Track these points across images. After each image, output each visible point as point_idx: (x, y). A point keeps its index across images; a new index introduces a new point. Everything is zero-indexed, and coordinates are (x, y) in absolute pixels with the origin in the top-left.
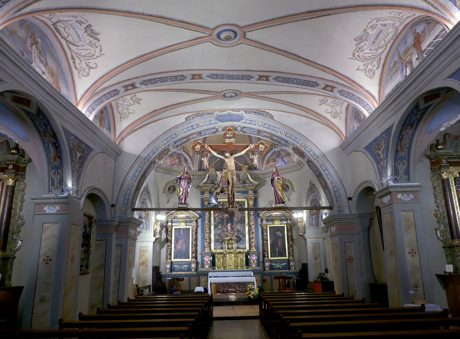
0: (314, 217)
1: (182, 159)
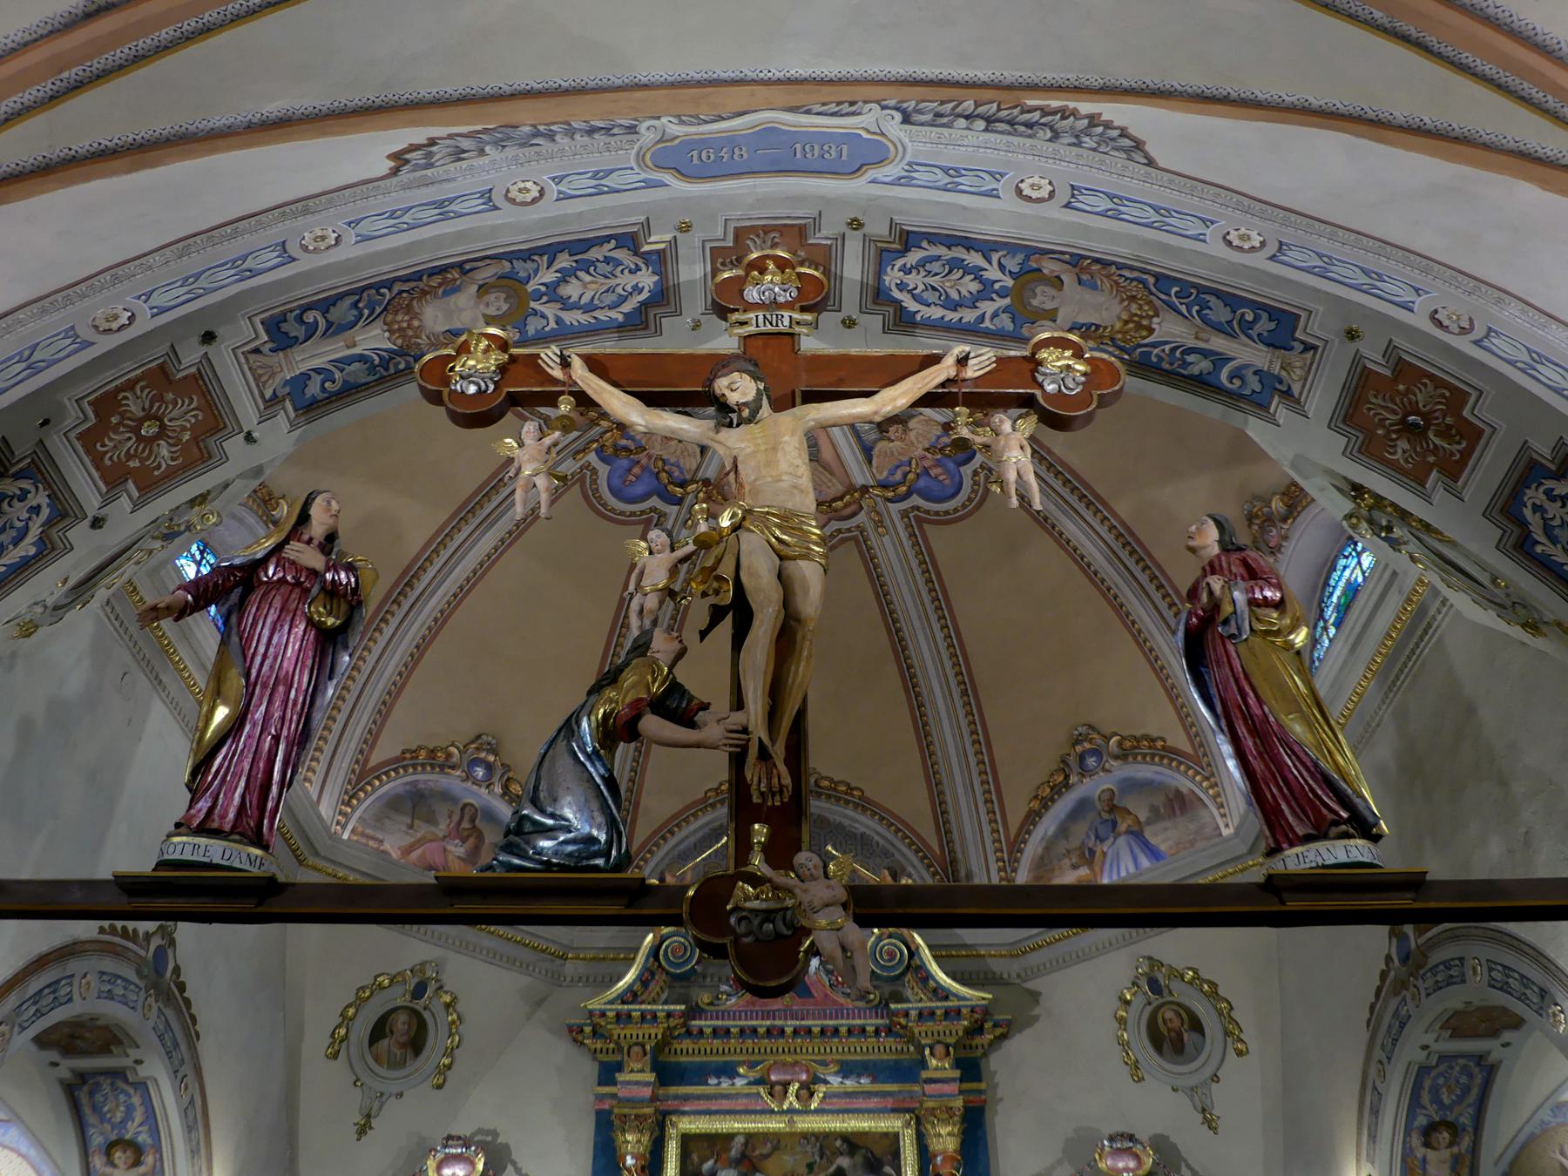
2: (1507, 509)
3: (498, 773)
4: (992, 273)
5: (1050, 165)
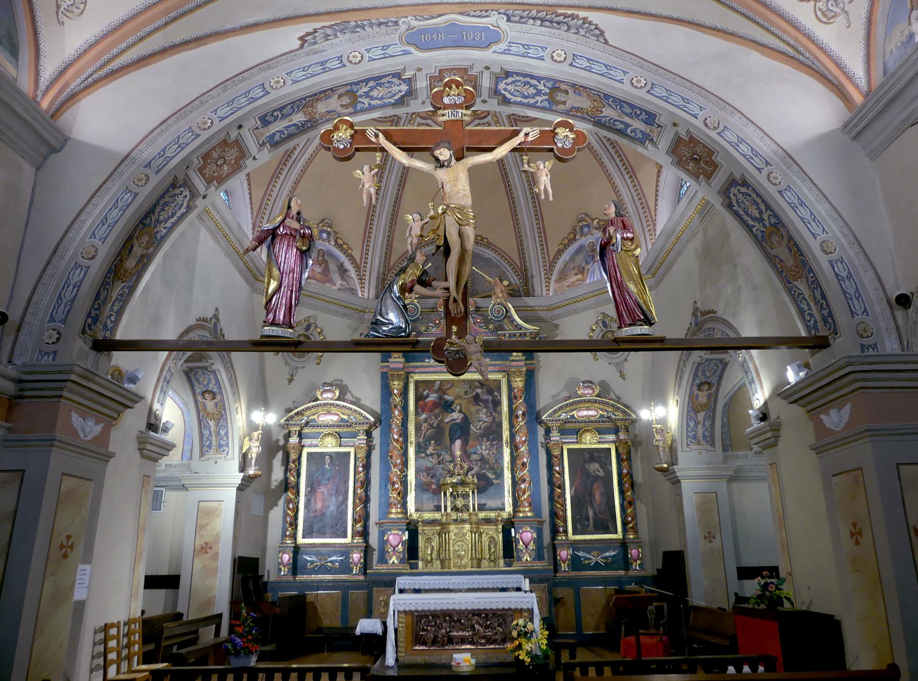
0: (701, 416)
1: (333, 267)
2: (725, 192)
3: (333, 235)
4: (541, 87)
5: (565, 43)
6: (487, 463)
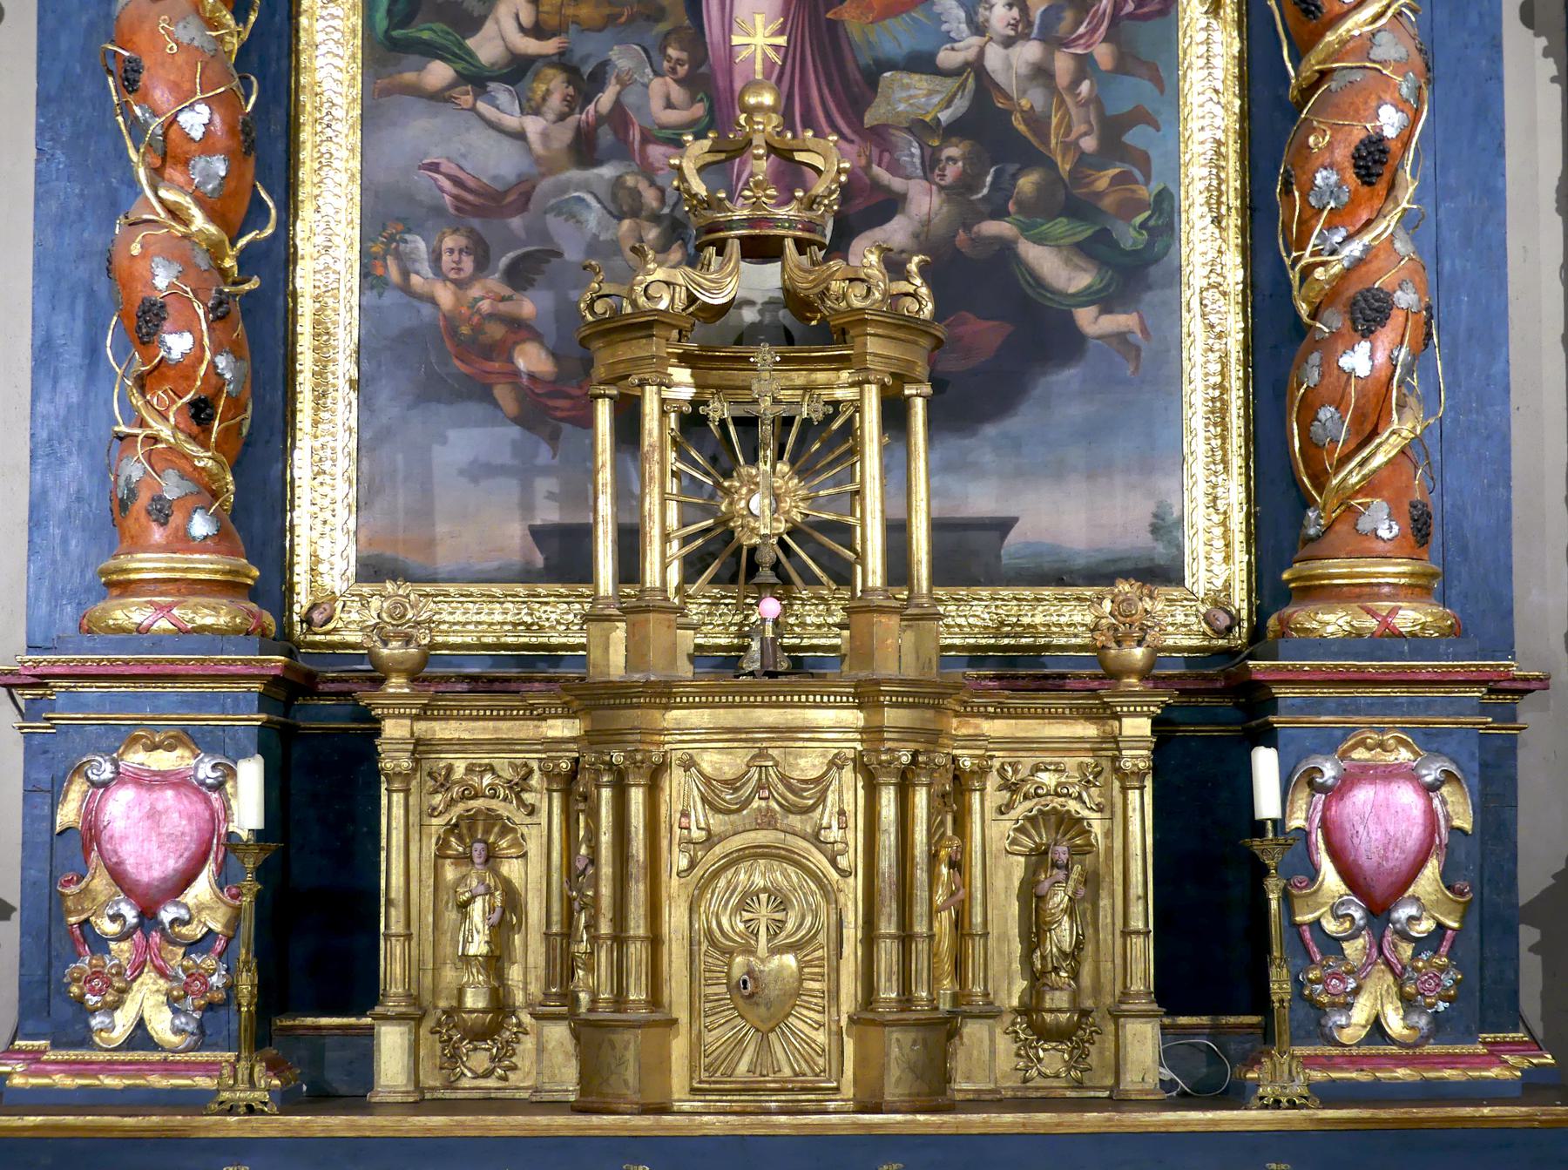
6: (1032, 157)
